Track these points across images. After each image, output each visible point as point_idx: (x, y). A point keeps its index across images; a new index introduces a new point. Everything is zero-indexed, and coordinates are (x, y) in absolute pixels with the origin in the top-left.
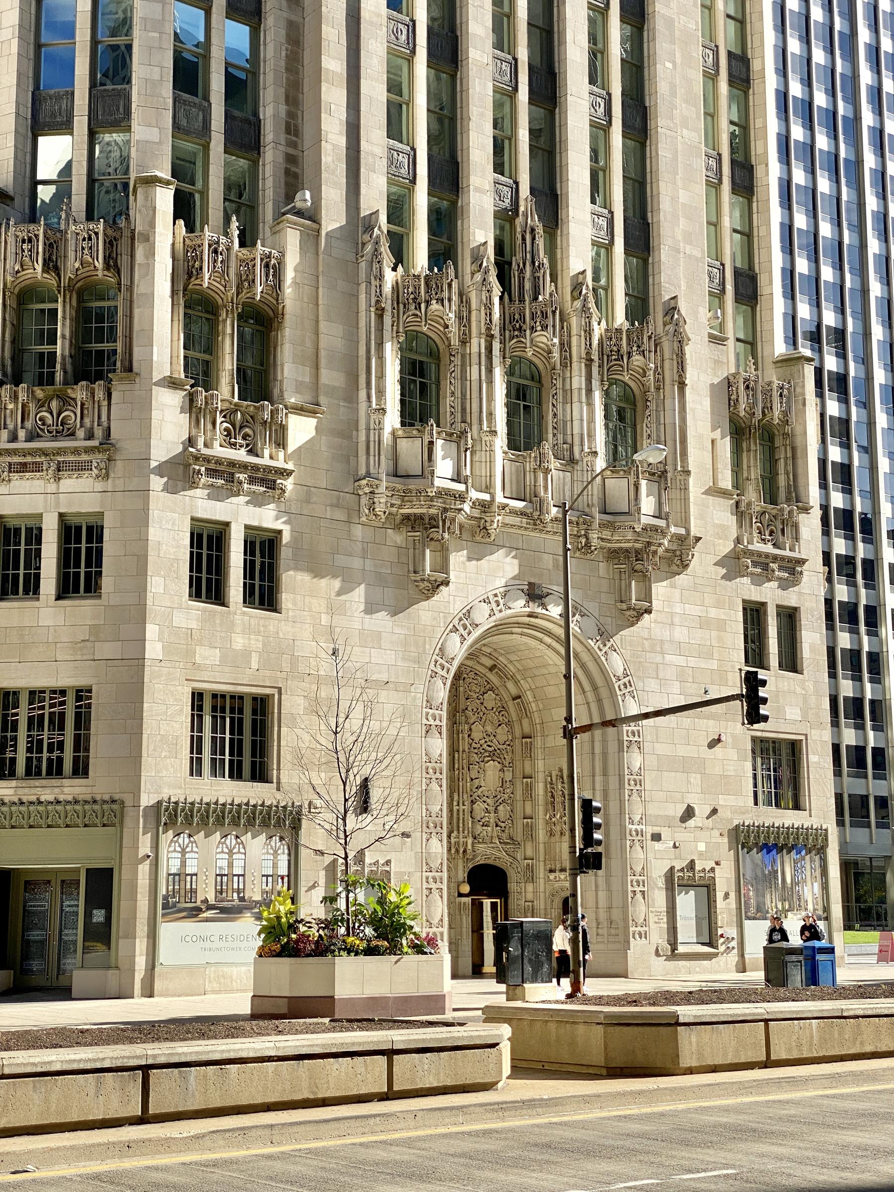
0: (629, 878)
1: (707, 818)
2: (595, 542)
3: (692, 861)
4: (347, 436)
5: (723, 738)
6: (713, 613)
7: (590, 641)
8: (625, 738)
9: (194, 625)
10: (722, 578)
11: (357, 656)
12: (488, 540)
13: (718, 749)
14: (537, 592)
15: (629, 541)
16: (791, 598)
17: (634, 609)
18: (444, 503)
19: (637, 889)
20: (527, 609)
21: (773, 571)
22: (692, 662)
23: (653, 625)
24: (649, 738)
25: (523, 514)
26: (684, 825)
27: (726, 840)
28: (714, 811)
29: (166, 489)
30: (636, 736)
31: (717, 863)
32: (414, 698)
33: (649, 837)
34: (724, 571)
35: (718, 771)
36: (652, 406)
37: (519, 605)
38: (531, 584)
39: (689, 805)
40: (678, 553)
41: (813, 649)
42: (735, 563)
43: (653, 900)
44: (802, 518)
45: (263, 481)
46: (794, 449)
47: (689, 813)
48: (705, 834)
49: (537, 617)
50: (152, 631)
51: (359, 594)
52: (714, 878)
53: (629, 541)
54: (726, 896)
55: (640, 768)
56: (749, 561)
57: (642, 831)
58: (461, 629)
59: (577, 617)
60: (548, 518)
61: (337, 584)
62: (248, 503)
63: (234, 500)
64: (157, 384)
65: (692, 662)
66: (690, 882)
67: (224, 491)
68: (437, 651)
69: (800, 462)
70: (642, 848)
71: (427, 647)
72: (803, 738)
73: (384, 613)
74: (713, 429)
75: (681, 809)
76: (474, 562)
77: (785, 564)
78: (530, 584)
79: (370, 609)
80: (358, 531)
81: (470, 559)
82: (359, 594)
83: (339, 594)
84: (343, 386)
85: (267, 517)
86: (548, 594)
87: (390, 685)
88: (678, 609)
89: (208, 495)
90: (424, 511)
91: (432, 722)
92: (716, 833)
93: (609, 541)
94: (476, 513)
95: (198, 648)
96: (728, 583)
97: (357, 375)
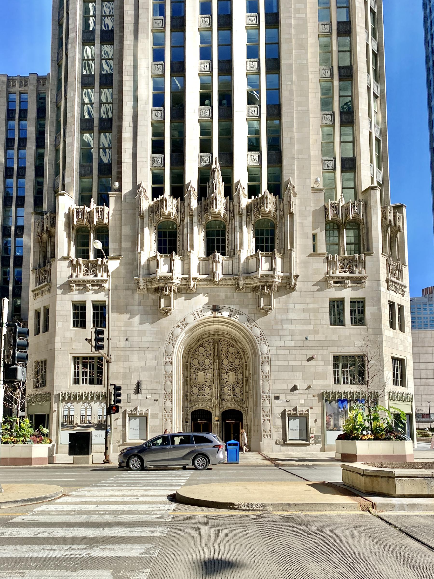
0: (262, 414)
1: (306, 390)
2: (241, 286)
3: (296, 407)
4: (133, 265)
5: (314, 357)
6: (311, 306)
7: (243, 324)
8: (261, 360)
9: (72, 335)
10: (317, 290)
11: (135, 339)
12: (193, 292)
13: (312, 362)
14: (217, 308)
15: (257, 283)
16: (358, 294)
17: (263, 309)
18: (164, 281)
19: (266, 418)
20: (212, 315)
21: (347, 283)
22: (298, 327)
23: (276, 314)
24: (273, 359)
25: (206, 280)
26: (292, 393)
27: (316, 398)
28: (309, 387)
29: (63, 293)
30: (267, 359)
31: (311, 408)
32: (160, 353)
33: (273, 398)
34: (319, 287)
35: (313, 370)
36: (279, 226)
37: (209, 314)
38: (213, 306)
39: (295, 385)
40: (287, 284)
41: (373, 314)
42: (324, 283)
43: (275, 423)
44: (368, 258)
45: (97, 285)
46: (367, 229)
47: (295, 388)
48: (305, 397)
49: (218, 318)
50: (57, 339)
51: (137, 319)
52: (308, 414)
53: (257, 283)
54: (316, 421)
55: (269, 371)
56: (332, 281)
57: (269, 396)
58: (181, 326)
59: (237, 315)
60: (217, 280)
61: (128, 316)
62: (93, 293)
63: (87, 293)
64: (59, 260)
65: (298, 327)
66: (295, 416)
67: (84, 291)
68: (170, 335)
69: (370, 233)
70: (269, 402)
71: (166, 334)
72: (365, 353)
73: (148, 324)
74: (314, 229)
75: (291, 387)
76: (188, 300)
77: (355, 280)
78: (213, 306)
79: (142, 322)
80: (136, 297)
81: (185, 300)
82: (137, 319)
83: (129, 319)
84: (130, 246)
85: (101, 297)
86: (222, 308)
87: (150, 349)
88: (291, 306)
89: (78, 293)
90: (158, 285)
91: (167, 360)
92: (311, 396)
93: (250, 284)
94: (184, 283)
95: (74, 343)
96: (321, 292)
97: (135, 243)
